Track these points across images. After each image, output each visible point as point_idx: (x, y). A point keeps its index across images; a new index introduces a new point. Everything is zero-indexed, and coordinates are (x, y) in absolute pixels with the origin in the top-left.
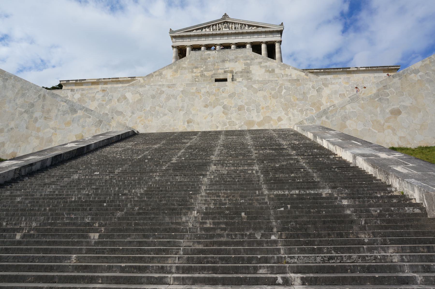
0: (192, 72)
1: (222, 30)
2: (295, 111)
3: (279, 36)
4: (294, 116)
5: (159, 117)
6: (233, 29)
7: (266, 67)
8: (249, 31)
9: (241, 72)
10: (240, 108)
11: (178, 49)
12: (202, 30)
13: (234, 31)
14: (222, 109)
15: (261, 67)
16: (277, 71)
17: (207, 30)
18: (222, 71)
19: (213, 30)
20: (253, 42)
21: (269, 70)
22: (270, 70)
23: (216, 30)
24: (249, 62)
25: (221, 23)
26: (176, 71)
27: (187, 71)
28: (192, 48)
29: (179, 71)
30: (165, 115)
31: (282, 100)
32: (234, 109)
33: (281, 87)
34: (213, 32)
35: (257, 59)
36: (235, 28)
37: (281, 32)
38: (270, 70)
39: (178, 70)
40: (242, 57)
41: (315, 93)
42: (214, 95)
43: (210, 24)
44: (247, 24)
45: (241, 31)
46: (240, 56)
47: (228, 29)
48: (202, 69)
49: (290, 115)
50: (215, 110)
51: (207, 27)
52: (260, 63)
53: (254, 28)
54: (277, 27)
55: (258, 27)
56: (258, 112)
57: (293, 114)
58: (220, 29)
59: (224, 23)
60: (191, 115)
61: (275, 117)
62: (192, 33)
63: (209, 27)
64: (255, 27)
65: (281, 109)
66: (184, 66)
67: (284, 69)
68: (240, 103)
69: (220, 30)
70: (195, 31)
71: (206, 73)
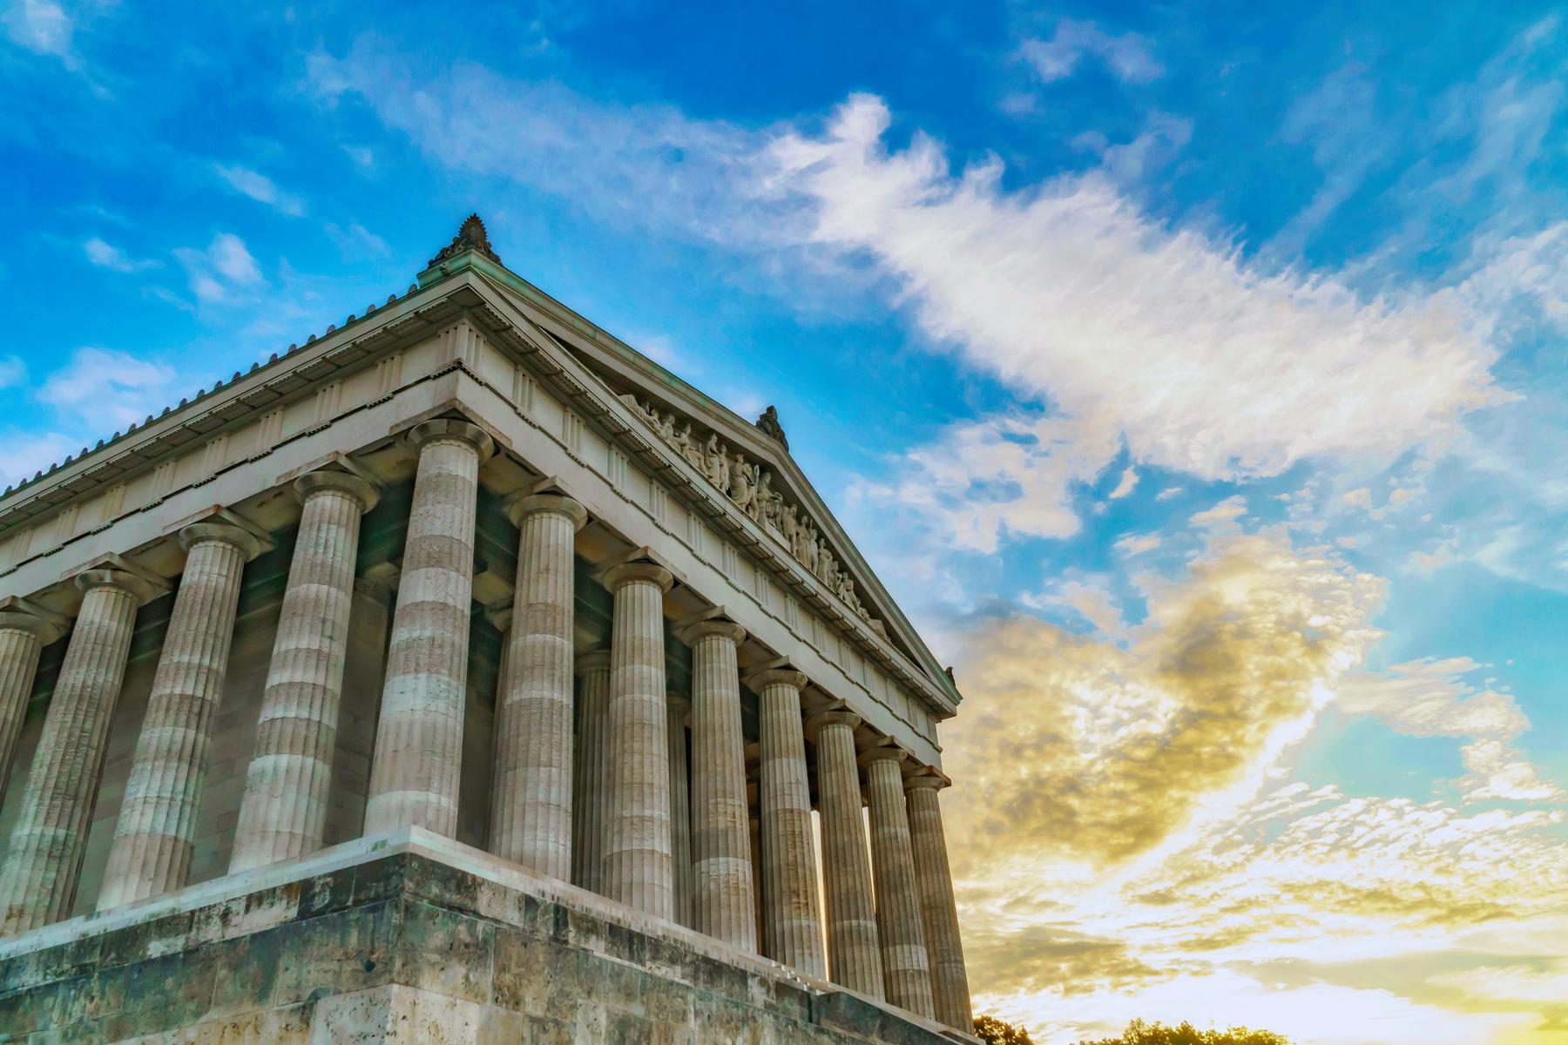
53: (871, 622)
62: (621, 411)
63: (702, 434)
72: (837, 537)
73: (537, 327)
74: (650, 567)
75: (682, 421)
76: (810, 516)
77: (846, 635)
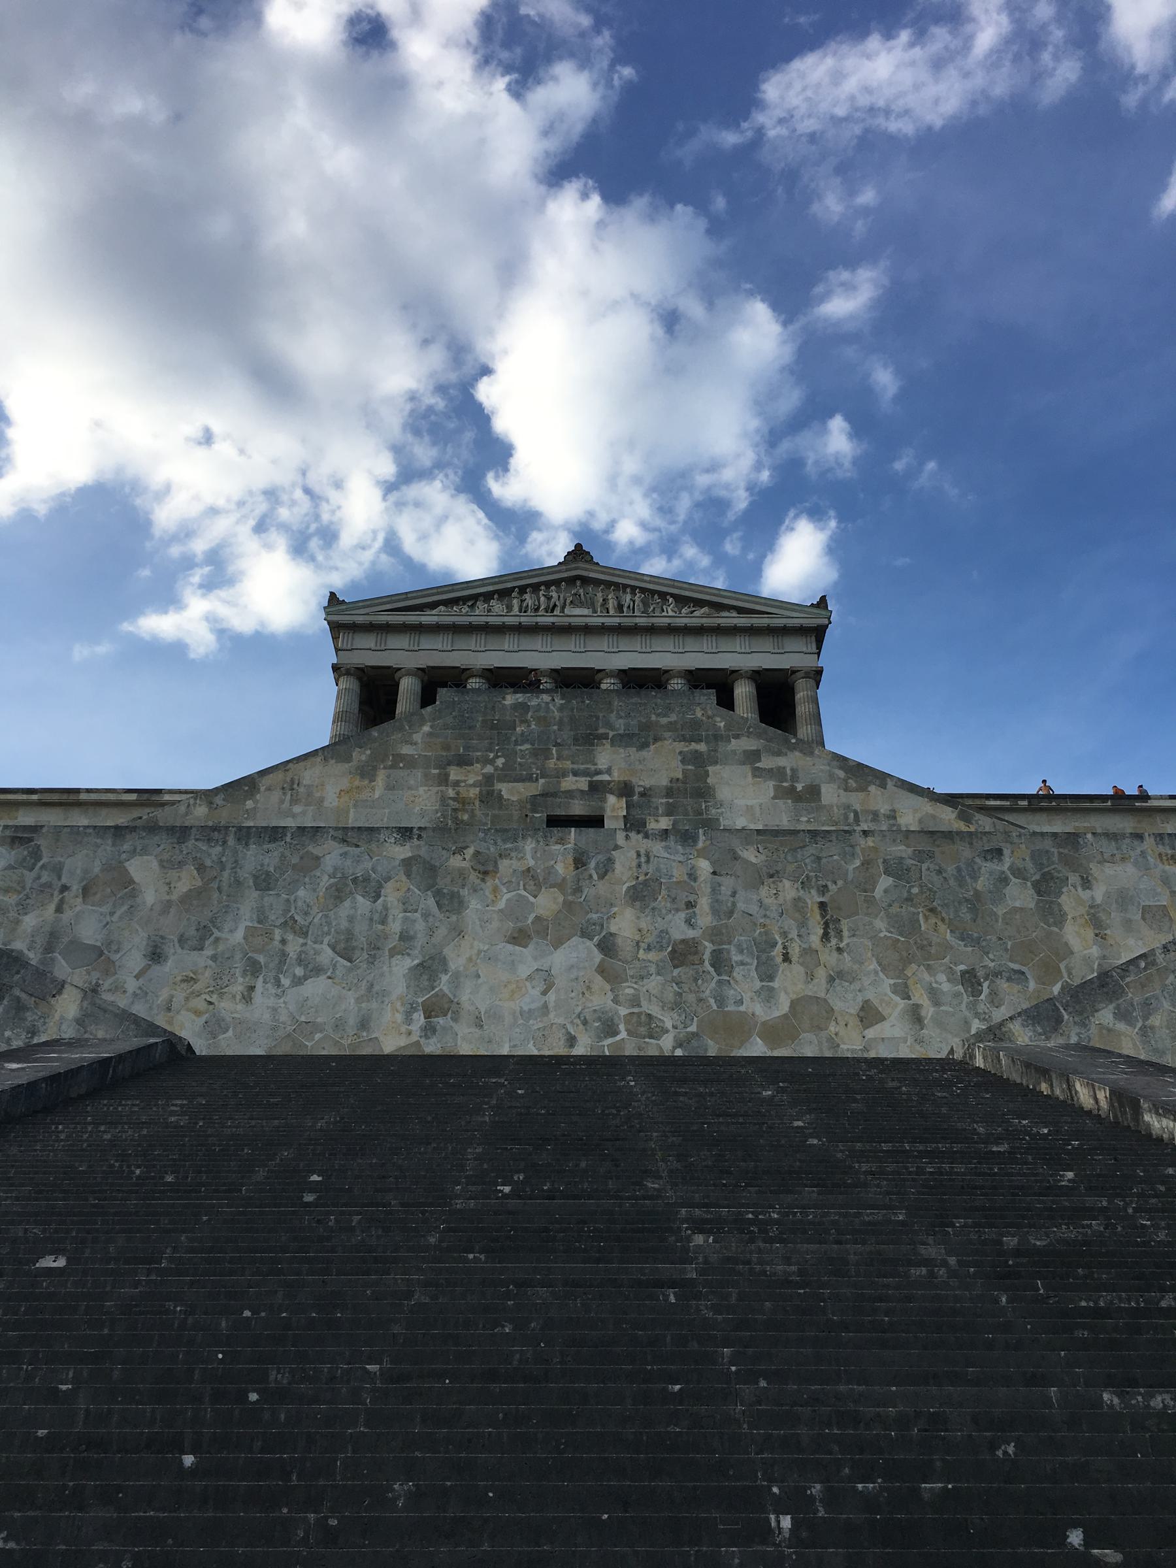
0: (444, 780)
1: (562, 611)
2: (942, 977)
3: (809, 650)
4: (937, 1003)
5: (286, 982)
6: (612, 612)
7: (777, 774)
8: (681, 622)
10: (683, 953)
11: (360, 679)
12: (472, 607)
14: (598, 957)
15: (758, 773)
17: (497, 606)
18: (583, 783)
19: (523, 609)
20: (697, 669)
21: (793, 788)
22: (799, 787)
23: (537, 610)
24: (702, 747)
25: (557, 583)
26: (366, 772)
27: (419, 774)
28: (422, 681)
29: (381, 777)
30: (318, 970)
31: (880, 924)
32: (652, 956)
33: (866, 864)
34: (522, 619)
35: (737, 737)
36: (620, 608)
37: (818, 634)
38: (799, 787)
39: (375, 768)
40: (671, 727)
42: (561, 886)
43: (509, 585)
44: (672, 595)
45: (642, 621)
46: (664, 721)
47: (586, 612)
48: (489, 769)
49: (920, 997)
50: (560, 959)
51: (496, 596)
52: (754, 756)
54: (800, 612)
55: (719, 607)
56: (767, 974)
57: (934, 995)
58: (555, 606)
59: (571, 581)
60: (445, 978)
61: (846, 1003)
64: (705, 610)
65: (873, 965)
66: (406, 750)
67: (863, 789)
68: (679, 930)
69: (552, 611)
70: (442, 608)
71: (506, 790)
72: (650, 582)
73: (368, 614)
74: (468, 672)
75: (488, 597)
76: (617, 585)
77: (671, 630)
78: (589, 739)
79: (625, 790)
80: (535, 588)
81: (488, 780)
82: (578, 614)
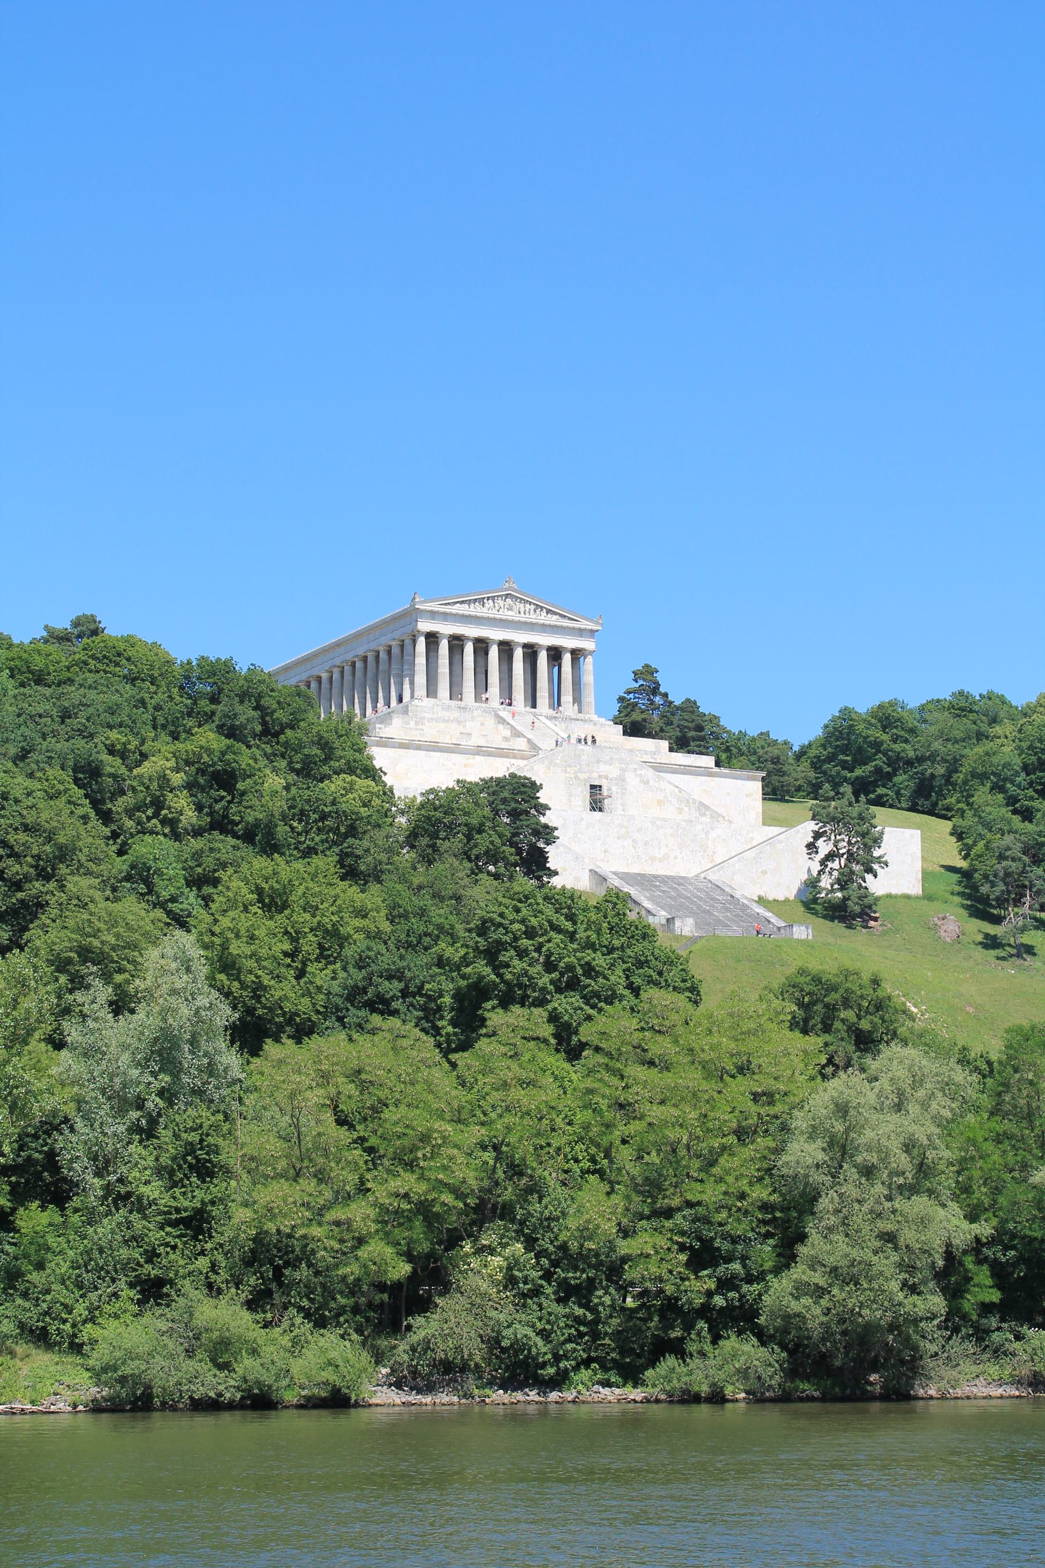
0: (566, 771)
9: (616, 779)
13: (522, 618)
16: (651, 783)
25: (501, 596)
41: (704, 836)
52: (635, 770)
78: (598, 762)
79: (606, 777)
80: (493, 598)
81: (576, 772)
82: (510, 615)
